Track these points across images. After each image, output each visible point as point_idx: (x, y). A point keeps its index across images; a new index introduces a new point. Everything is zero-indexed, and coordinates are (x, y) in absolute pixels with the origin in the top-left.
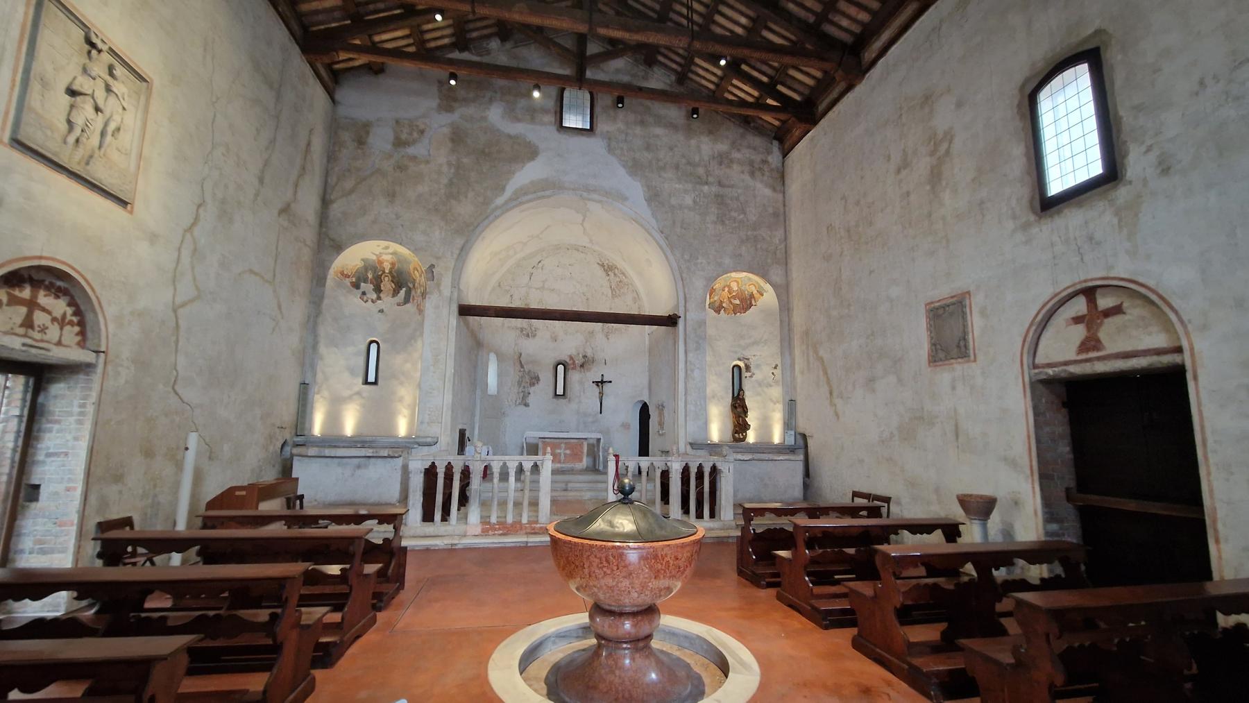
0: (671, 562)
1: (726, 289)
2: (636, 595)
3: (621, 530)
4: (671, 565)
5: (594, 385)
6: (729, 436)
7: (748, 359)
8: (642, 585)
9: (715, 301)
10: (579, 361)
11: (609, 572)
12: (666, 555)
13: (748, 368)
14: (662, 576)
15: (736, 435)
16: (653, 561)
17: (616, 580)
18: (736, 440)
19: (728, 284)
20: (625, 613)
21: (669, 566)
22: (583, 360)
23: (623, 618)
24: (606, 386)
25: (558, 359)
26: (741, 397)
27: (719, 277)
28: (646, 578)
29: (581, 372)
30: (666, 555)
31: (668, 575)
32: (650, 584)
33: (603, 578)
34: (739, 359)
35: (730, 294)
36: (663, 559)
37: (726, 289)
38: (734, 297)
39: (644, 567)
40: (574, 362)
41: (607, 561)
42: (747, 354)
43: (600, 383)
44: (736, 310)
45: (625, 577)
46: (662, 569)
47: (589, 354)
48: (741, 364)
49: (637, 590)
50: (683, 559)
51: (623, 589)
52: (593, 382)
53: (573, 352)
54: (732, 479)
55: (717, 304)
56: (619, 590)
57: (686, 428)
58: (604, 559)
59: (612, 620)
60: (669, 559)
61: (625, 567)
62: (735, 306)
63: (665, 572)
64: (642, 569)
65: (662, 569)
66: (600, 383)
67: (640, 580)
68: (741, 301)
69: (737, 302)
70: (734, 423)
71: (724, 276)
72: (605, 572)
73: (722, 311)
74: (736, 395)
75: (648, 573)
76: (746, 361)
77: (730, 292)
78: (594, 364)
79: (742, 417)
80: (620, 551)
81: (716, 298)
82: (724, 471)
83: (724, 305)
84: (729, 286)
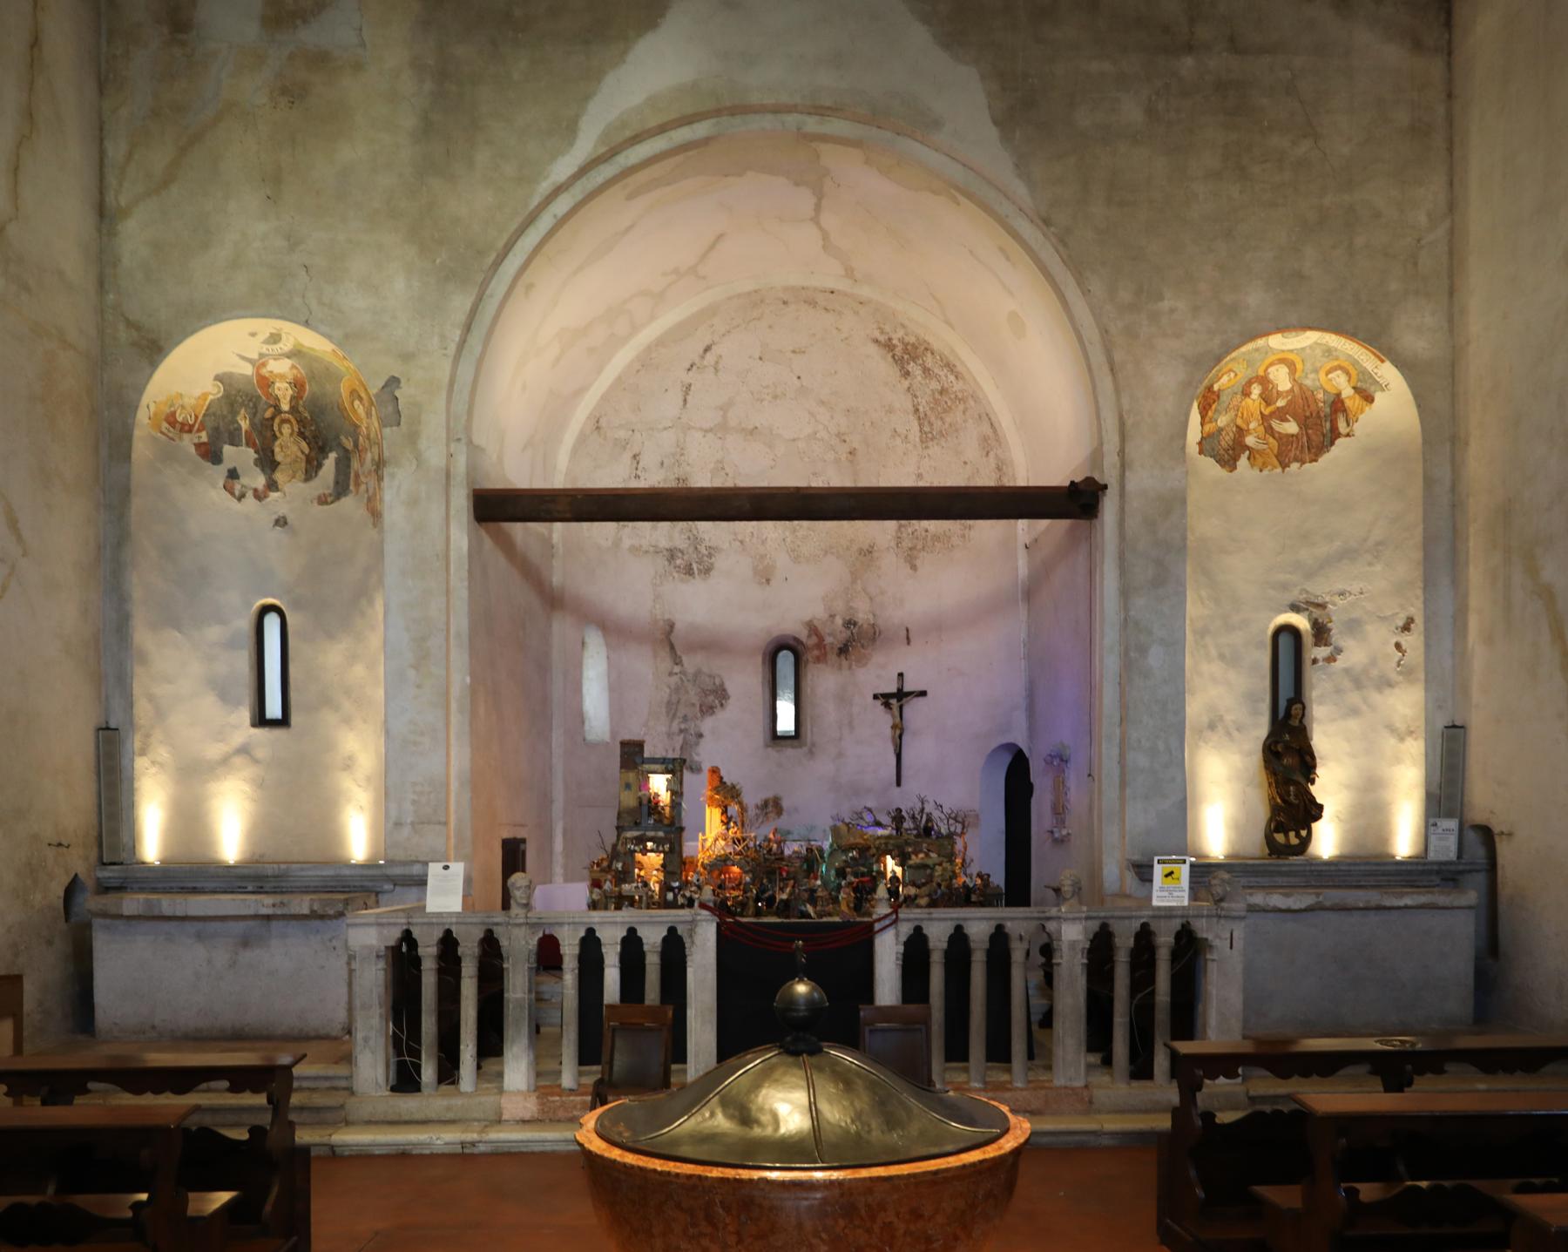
1: (1256, 390)
5: (878, 703)
6: (1255, 844)
7: (1322, 606)
9: (1220, 430)
10: (835, 634)
13: (1321, 632)
15: (1280, 837)
18: (1275, 849)
19: (1261, 373)
22: (846, 634)
24: (913, 709)
25: (776, 633)
26: (1295, 723)
27: (1228, 353)
29: (840, 668)
34: (1295, 608)
35: (1268, 404)
37: (1256, 390)
38: (1281, 415)
40: (821, 639)
42: (1320, 589)
43: (896, 699)
44: (1288, 453)
47: (862, 617)
48: (1301, 622)
52: (875, 697)
53: (817, 612)
55: (1227, 439)
62: (1285, 440)
66: (896, 699)
68: (1304, 423)
69: (1291, 427)
70: (1272, 799)
71: (1243, 349)
73: (1243, 462)
74: (1281, 714)
76: (1317, 612)
77: (1267, 399)
78: (878, 643)
79: (1297, 784)
81: (1222, 421)
82: (1216, 943)
83: (1250, 440)
84: (1264, 381)
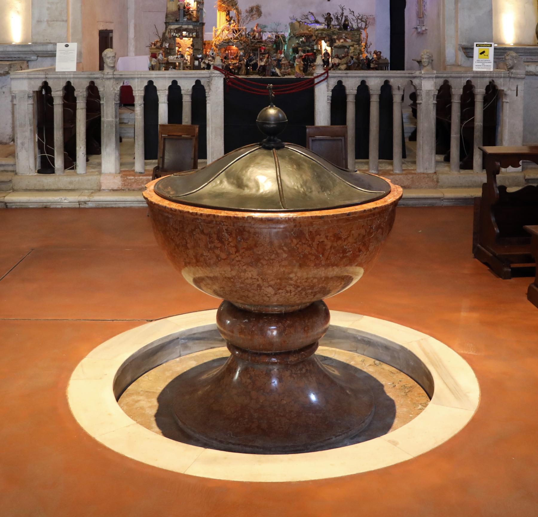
0: (329, 244)
2: (270, 290)
3: (254, 191)
4: (328, 247)
8: (280, 276)
11: (223, 255)
12: (318, 233)
14: (313, 265)
16: (295, 241)
17: (237, 268)
20: (267, 315)
21: (324, 250)
23: (261, 322)
28: (284, 266)
30: (318, 233)
31: (323, 263)
32: (291, 276)
33: (216, 264)
36: (313, 239)
39: (279, 251)
41: (220, 239)
45: (249, 264)
46: (310, 254)
49: (272, 283)
50: (350, 240)
51: (249, 281)
54: (521, 107)
56: (242, 283)
57: (457, 22)
58: (215, 236)
59: (244, 323)
60: (322, 238)
61: (249, 249)
63: (317, 257)
64: (277, 254)
65: (310, 254)
67: (275, 270)
72: (218, 256)
75: (285, 259)
80: (240, 224)
